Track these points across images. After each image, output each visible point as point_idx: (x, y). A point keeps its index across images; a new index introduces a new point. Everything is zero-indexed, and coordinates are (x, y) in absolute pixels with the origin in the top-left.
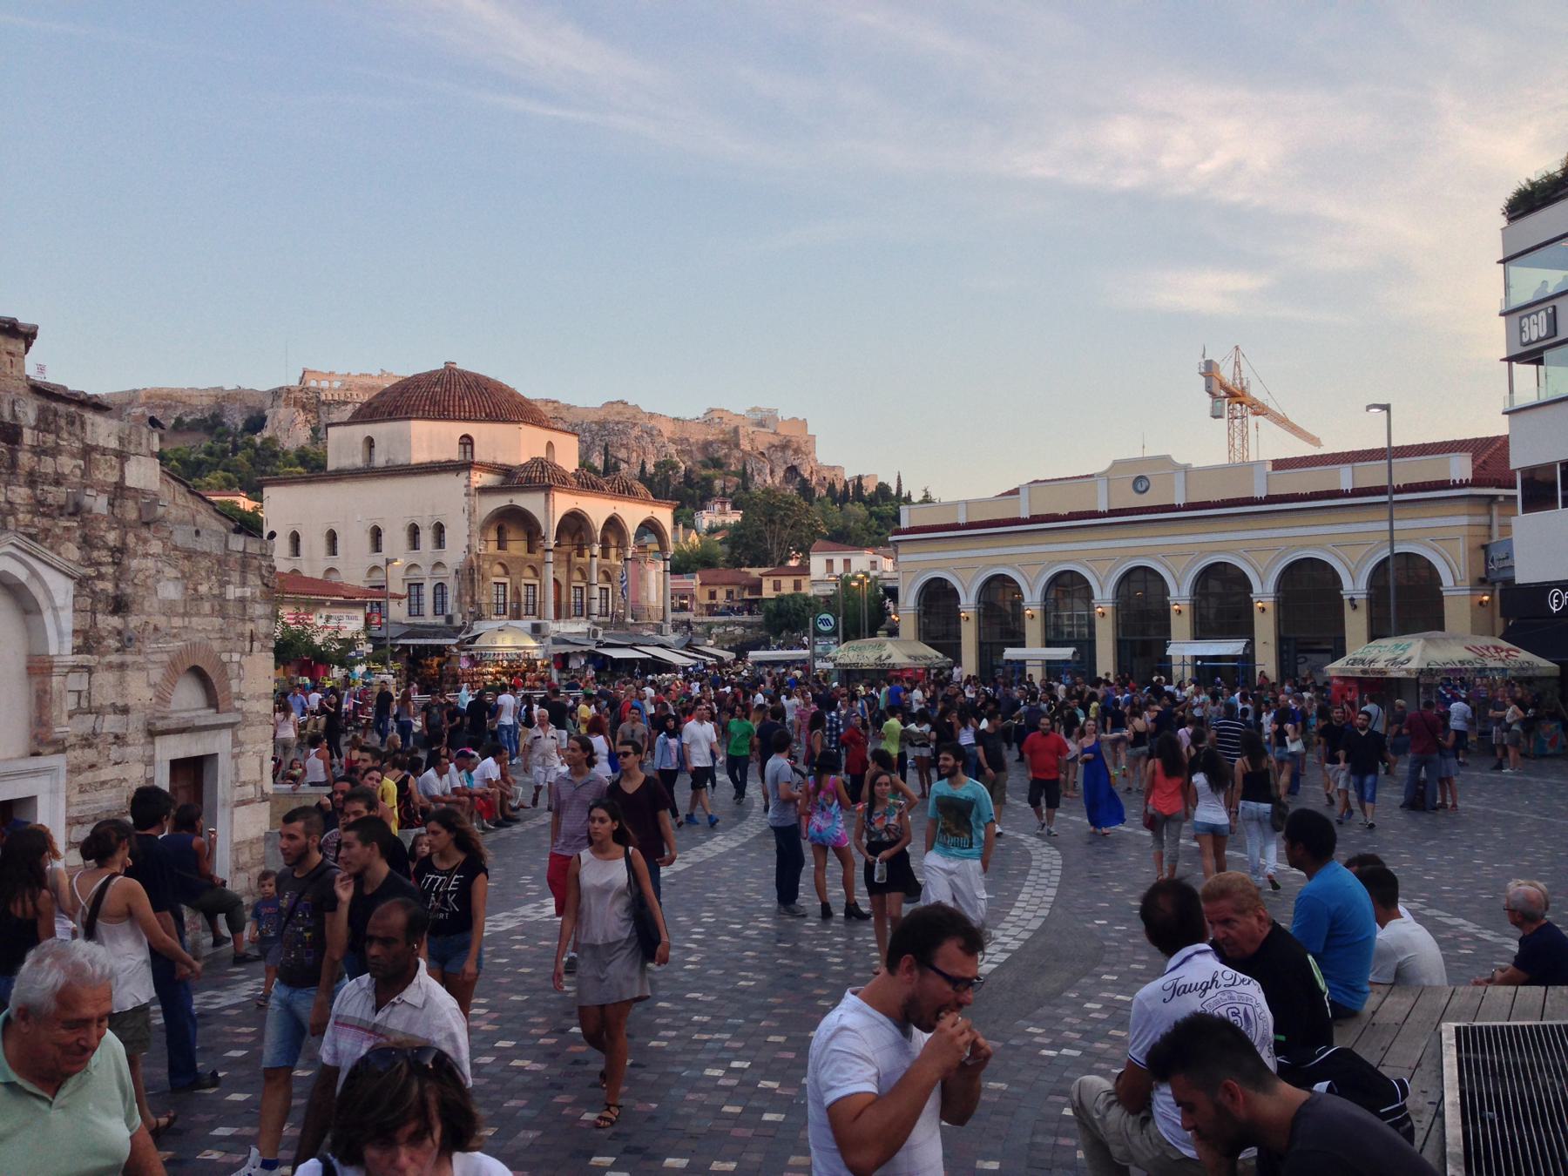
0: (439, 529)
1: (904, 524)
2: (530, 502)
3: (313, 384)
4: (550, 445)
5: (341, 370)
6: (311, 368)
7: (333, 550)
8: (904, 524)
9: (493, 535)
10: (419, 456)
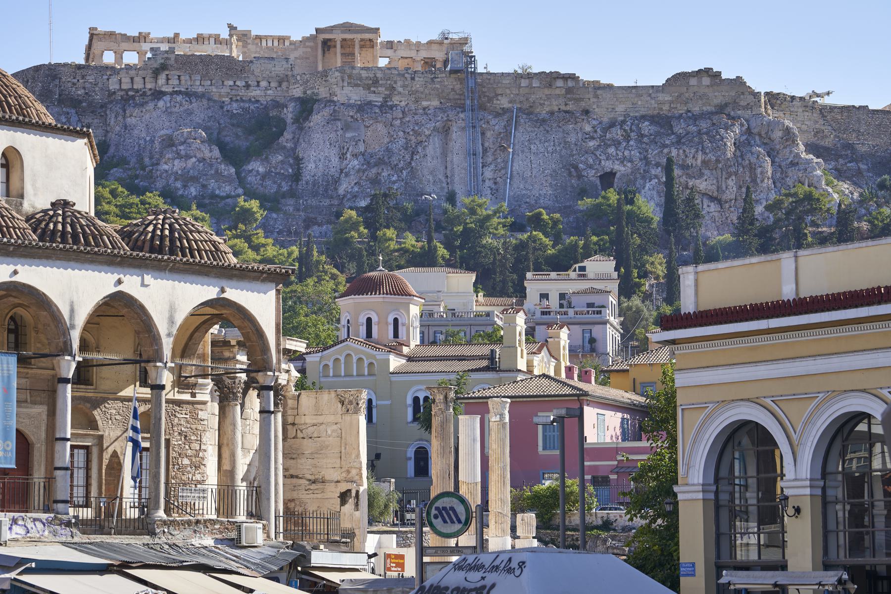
1: (688, 304)
3: (109, 58)
5: (160, 30)
6: (102, 28)
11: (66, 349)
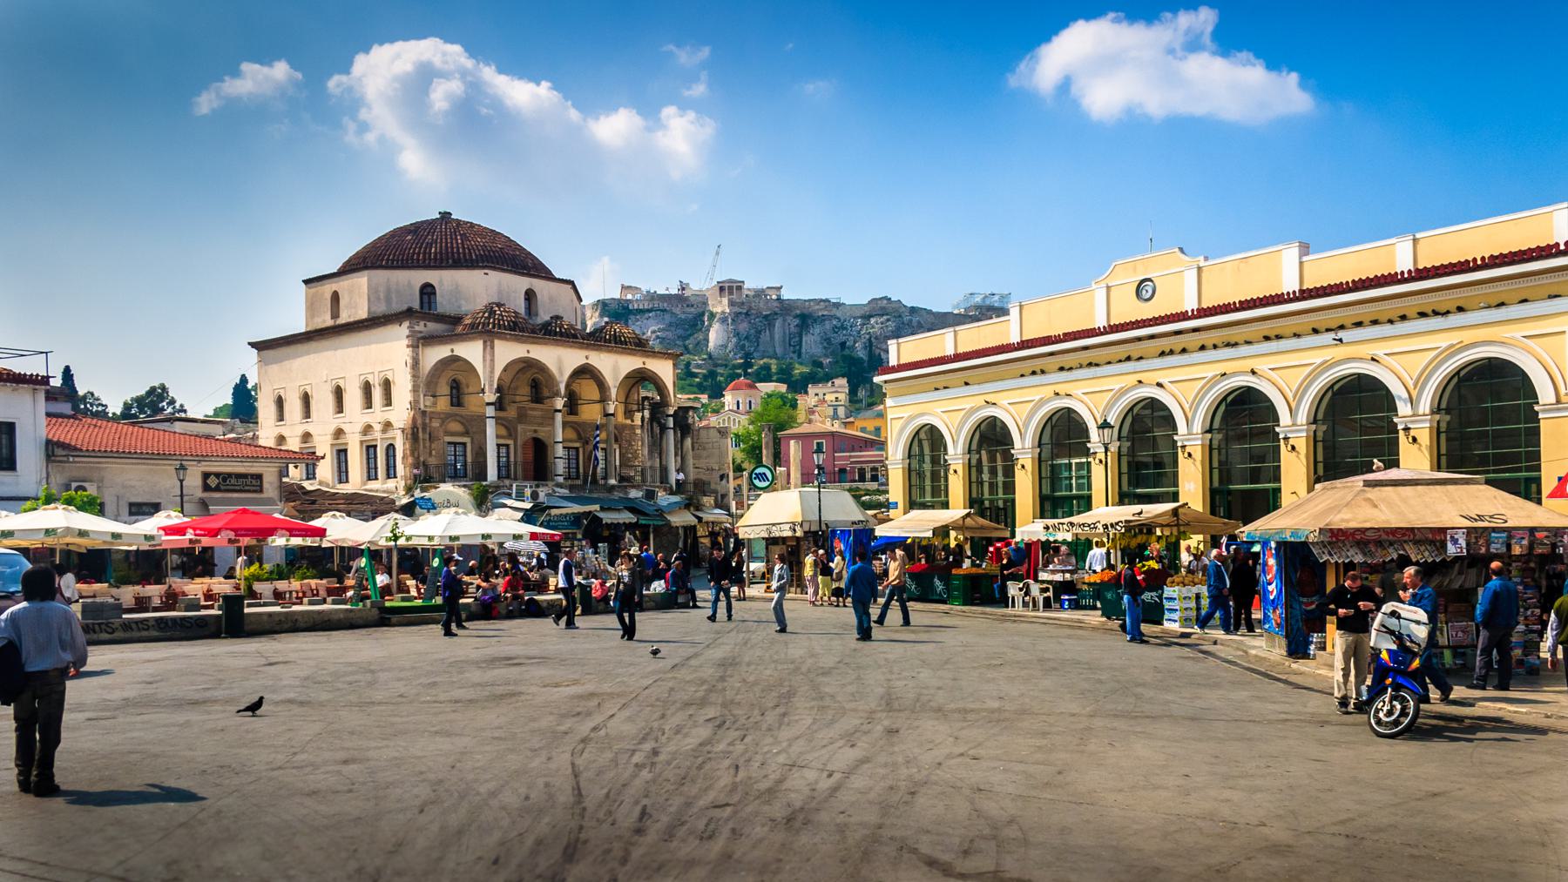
0: (387, 385)
1: (893, 362)
2: (471, 351)
3: (629, 297)
4: (530, 295)
7: (307, 413)
8: (893, 362)
9: (444, 389)
10: (381, 309)
11: (557, 394)
